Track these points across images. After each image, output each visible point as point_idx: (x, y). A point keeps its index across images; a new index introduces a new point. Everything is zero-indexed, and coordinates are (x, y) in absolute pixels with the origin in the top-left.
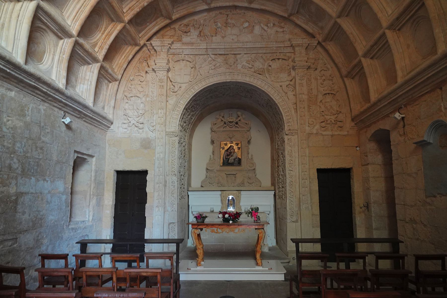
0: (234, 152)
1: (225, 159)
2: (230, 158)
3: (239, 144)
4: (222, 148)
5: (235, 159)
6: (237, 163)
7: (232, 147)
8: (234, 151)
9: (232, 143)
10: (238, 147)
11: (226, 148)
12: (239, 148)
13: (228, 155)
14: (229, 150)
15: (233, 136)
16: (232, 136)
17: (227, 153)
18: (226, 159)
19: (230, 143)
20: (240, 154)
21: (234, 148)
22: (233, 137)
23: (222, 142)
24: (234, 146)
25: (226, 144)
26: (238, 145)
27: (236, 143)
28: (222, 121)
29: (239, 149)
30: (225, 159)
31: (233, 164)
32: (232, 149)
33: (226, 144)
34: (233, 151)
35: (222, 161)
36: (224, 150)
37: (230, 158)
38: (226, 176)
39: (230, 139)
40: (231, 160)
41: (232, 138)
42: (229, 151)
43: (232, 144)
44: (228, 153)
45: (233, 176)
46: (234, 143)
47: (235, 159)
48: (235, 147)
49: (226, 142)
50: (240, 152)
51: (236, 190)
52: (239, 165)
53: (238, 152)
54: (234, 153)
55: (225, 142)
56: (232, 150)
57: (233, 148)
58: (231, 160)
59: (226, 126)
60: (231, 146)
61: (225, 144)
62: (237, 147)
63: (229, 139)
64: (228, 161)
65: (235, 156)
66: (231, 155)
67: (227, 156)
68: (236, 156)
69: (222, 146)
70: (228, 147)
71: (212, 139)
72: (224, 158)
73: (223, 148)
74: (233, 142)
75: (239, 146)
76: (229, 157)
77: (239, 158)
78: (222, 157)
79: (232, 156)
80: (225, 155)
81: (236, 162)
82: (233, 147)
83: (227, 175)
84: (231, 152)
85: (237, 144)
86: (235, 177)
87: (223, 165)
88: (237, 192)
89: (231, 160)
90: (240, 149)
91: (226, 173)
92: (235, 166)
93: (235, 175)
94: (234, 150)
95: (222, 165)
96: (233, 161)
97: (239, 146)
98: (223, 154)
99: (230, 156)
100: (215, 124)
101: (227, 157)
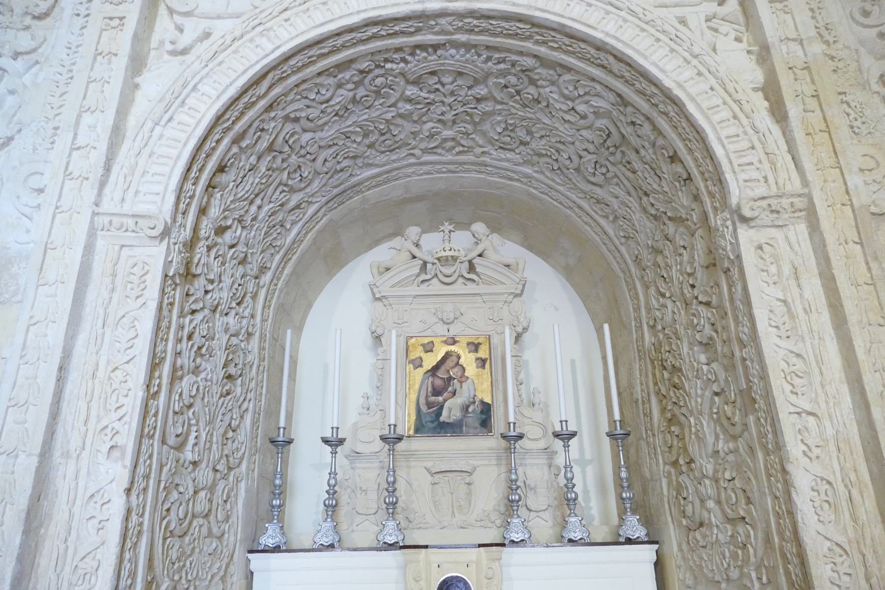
0: (463, 378)
1: (424, 409)
2: (447, 405)
3: (479, 344)
4: (412, 362)
5: (467, 407)
6: (477, 425)
7: (454, 359)
8: (463, 375)
9: (454, 342)
10: (477, 359)
11: (430, 362)
12: (482, 363)
13: (437, 392)
14: (443, 368)
15: (458, 314)
16: (452, 316)
17: (432, 383)
18: (429, 405)
19: (446, 342)
20: (486, 385)
21: (462, 361)
22: (456, 318)
23: (413, 341)
24: (461, 352)
25: (429, 348)
26: (476, 350)
27: (469, 344)
28: (414, 257)
29: (483, 367)
30: (424, 409)
31: (461, 426)
32: (452, 364)
33: (428, 348)
34: (459, 374)
35: (413, 417)
36: (421, 371)
37: (445, 401)
38: (430, 478)
39: (446, 327)
40: (450, 410)
41: (453, 322)
42: (441, 374)
43: (452, 348)
44: (438, 382)
45: (458, 477)
46: (464, 341)
47: (465, 408)
48: (468, 360)
49: (429, 339)
50: (485, 376)
51: (480, 546)
52: (486, 430)
53: (478, 375)
54: (461, 382)
55: (426, 341)
56: (456, 370)
57: (457, 364)
58: (451, 411)
59: (428, 277)
60: (447, 355)
61: (423, 345)
62: (472, 356)
63: (441, 329)
64: (439, 413)
65: (466, 395)
66: (450, 389)
67: (433, 395)
68: (472, 396)
69: (414, 355)
70: (439, 358)
71: (373, 328)
72: (422, 401)
73: (417, 364)
74: (457, 339)
75: (483, 353)
76: (440, 399)
77: (482, 402)
78: (413, 397)
79: (454, 393)
80: (424, 388)
81: (473, 420)
82: (459, 357)
83: (432, 475)
84: (450, 379)
85: (475, 347)
86: (469, 484)
87: (417, 430)
88: (484, 554)
89: (451, 411)
90: (487, 365)
91: (429, 464)
92: (467, 435)
93: (470, 473)
94: (464, 369)
95: (412, 432)
96: (456, 415)
97: (483, 353)
98: (417, 386)
99: (445, 394)
100: (388, 269)
101: (433, 399)
